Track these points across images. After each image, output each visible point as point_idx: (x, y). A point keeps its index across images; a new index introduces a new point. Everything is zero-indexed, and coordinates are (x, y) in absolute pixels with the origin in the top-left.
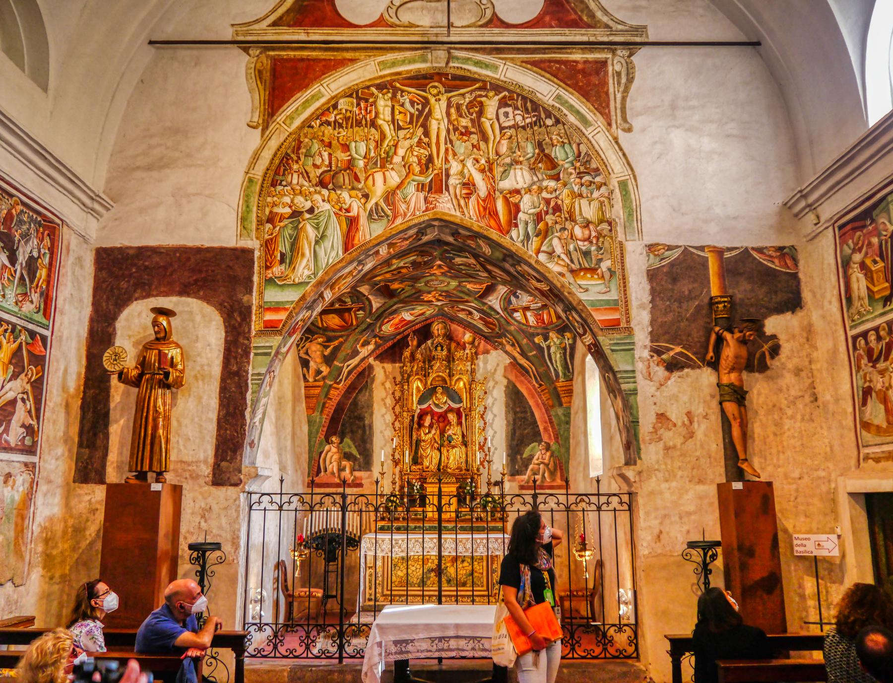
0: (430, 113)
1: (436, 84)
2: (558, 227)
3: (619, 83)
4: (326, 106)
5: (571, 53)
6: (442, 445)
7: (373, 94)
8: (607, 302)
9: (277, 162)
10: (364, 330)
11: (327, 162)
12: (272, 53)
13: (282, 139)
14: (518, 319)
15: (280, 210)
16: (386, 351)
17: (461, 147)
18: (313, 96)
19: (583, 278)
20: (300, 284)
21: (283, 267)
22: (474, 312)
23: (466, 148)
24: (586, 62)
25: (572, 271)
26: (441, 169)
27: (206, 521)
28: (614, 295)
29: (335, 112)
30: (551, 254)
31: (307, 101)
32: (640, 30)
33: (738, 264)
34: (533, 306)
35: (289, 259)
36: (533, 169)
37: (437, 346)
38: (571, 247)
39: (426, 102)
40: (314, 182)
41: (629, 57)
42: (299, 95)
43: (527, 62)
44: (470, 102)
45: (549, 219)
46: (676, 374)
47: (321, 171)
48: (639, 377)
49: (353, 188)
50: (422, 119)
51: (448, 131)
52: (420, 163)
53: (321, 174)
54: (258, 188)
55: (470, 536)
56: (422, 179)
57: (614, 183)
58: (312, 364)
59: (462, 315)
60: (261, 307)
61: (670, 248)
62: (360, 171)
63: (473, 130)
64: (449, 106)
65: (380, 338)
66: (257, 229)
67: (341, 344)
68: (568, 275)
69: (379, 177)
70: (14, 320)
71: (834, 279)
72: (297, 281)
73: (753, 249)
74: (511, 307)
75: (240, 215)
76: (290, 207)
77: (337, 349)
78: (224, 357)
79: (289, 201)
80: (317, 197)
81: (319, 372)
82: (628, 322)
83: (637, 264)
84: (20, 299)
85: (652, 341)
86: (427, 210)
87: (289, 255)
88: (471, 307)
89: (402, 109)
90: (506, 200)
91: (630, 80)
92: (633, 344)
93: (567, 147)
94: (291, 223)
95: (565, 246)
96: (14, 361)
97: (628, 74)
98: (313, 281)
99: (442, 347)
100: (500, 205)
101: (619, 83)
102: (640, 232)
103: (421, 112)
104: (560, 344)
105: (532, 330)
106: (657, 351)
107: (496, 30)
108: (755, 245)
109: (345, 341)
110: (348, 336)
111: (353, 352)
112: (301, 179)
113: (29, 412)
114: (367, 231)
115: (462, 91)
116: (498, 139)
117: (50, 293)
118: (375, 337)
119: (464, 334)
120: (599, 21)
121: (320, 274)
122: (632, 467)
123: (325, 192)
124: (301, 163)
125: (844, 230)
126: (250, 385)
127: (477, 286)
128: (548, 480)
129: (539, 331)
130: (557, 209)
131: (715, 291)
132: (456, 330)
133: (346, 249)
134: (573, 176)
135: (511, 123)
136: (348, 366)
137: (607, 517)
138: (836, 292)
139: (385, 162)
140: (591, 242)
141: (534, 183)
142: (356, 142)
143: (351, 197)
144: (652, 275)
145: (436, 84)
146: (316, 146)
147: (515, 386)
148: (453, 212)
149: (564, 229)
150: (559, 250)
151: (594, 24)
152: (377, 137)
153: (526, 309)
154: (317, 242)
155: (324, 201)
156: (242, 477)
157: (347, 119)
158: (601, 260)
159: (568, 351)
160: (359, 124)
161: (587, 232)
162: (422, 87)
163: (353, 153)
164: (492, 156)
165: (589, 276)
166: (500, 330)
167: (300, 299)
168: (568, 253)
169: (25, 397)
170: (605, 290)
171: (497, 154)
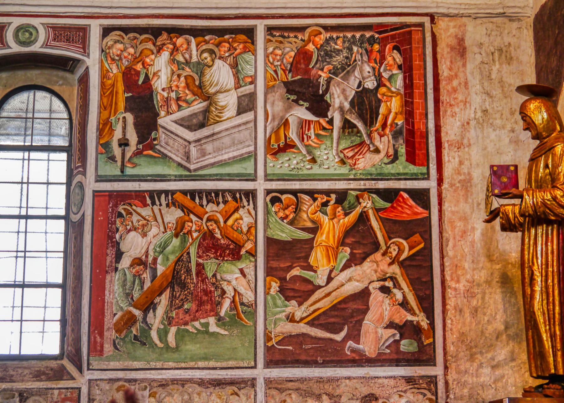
70: (341, 185)
84: (350, 154)
96: (349, 241)
113: (404, 304)
117: (419, 126)
169: (389, 284)
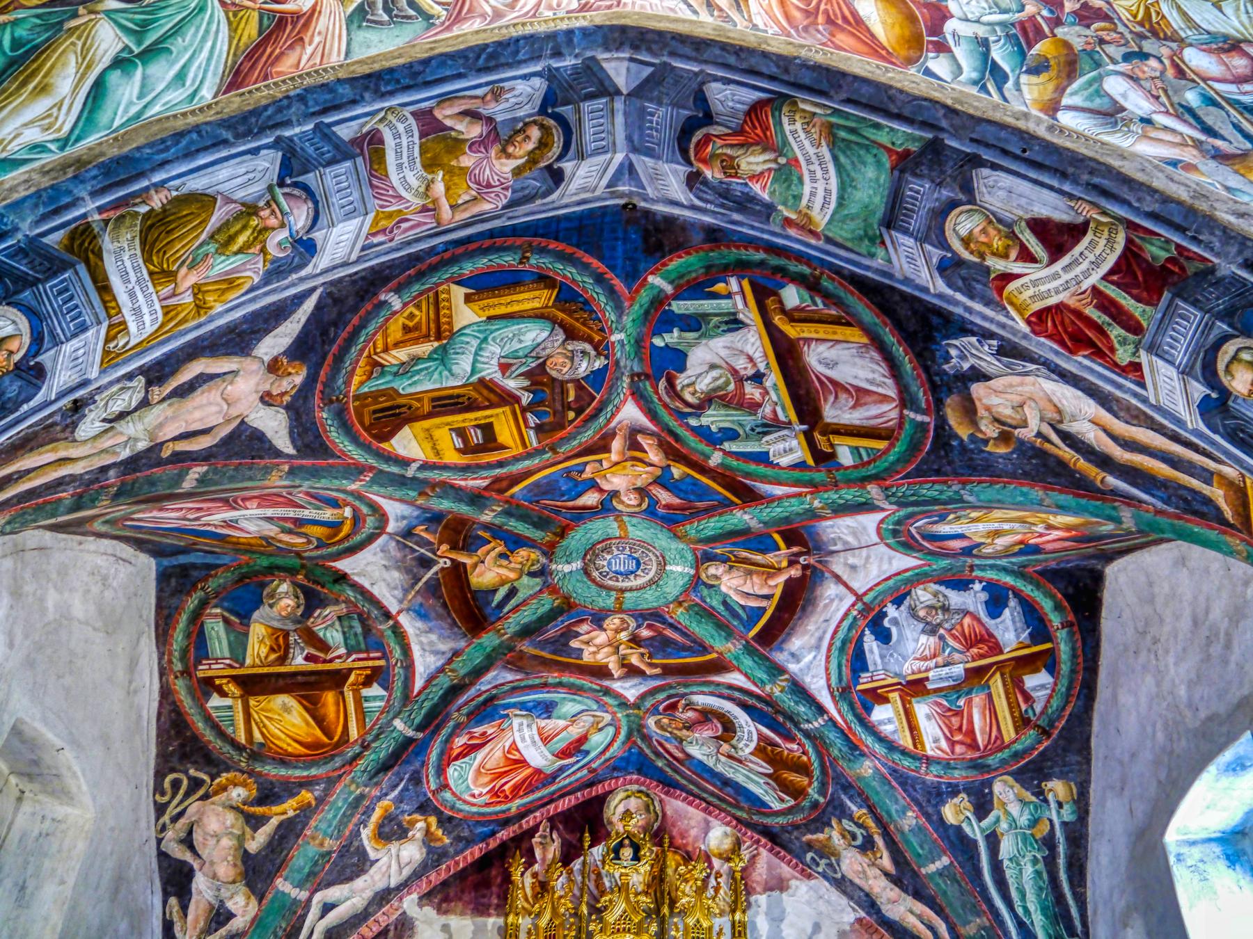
10: (385, 767)
14: (887, 729)
16: (462, 875)
22: (742, 718)
30: (1112, 114)
34: (938, 676)
37: (621, 845)
58: (200, 883)
59: (700, 748)
65: (444, 821)
67: (306, 812)
74: (865, 683)
77: (289, 832)
81: (220, 916)
88: (731, 692)
99: (637, 849)
104: (1034, 822)
105: (931, 775)
109: (320, 801)
110: (331, 782)
111: (344, 851)
118: (424, 808)
119: (707, 829)
127: (755, 585)
129: (958, 775)
132: (680, 815)
136: (327, 908)
153: (915, 687)
159: (1061, 849)
166: (822, 792)
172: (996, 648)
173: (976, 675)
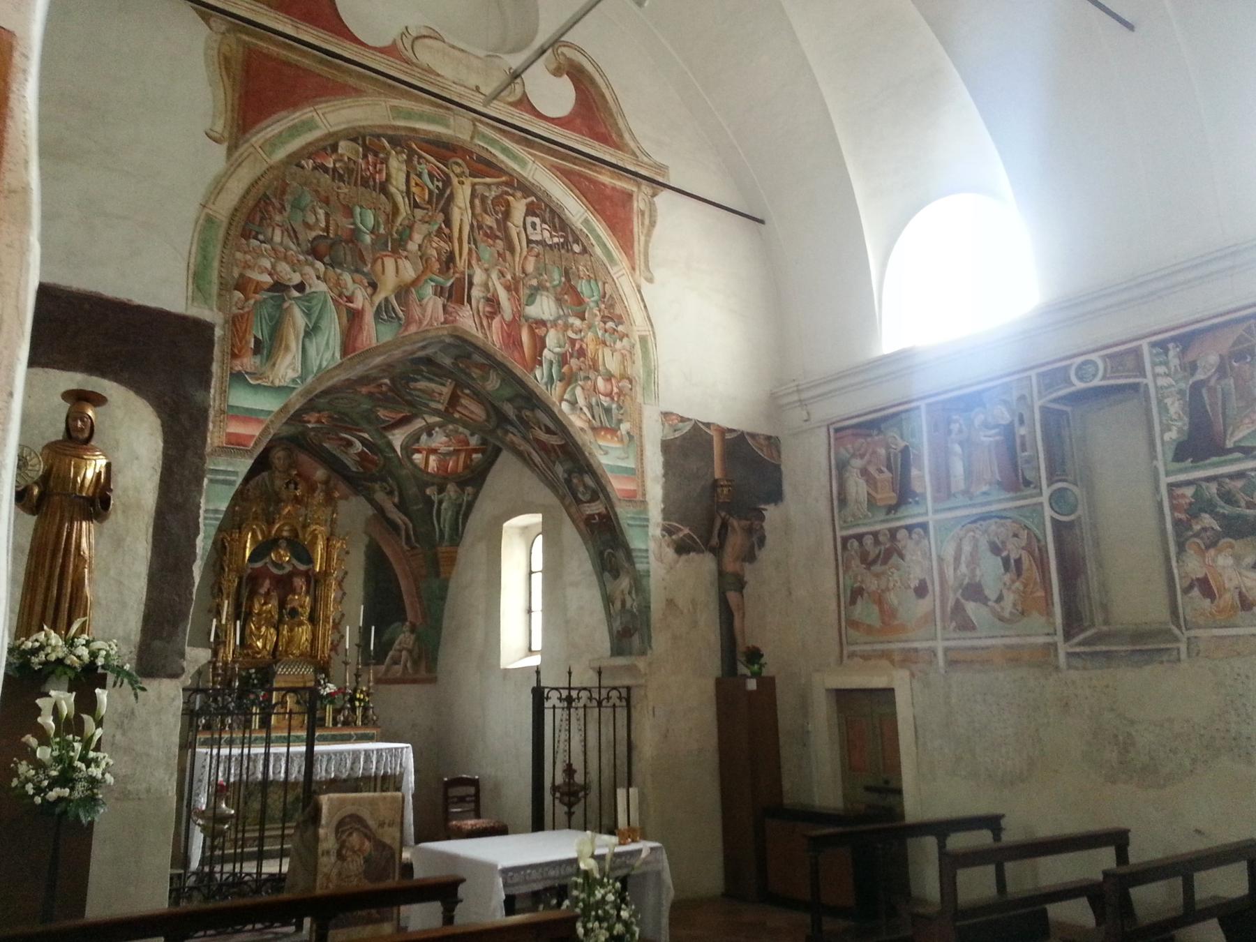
0: (451, 198)
1: (460, 161)
2: (582, 374)
3: (643, 224)
4: (322, 144)
5: (600, 173)
6: (281, 621)
7: (384, 148)
8: (626, 469)
9: (251, 203)
11: (323, 225)
12: (245, 38)
13: (258, 172)
14: (417, 461)
15: (255, 276)
17: (487, 252)
18: (304, 123)
19: (604, 438)
20: (280, 389)
21: (257, 360)
23: (491, 255)
24: (614, 188)
25: (593, 429)
26: (463, 273)
27: (124, 734)
28: (631, 464)
29: (334, 157)
31: (294, 127)
32: (662, 168)
33: (739, 446)
35: (268, 348)
36: (559, 301)
38: (594, 401)
39: (447, 182)
40: (305, 248)
41: (654, 195)
42: (283, 113)
43: (558, 169)
44: (496, 197)
45: (574, 362)
46: (684, 557)
47: (314, 234)
48: (652, 558)
49: (357, 271)
50: (443, 201)
51: (472, 226)
52: (439, 260)
53: (314, 239)
54: (221, 233)
55: (284, 750)
56: (440, 279)
57: (635, 337)
60: (223, 412)
61: (683, 420)
62: (366, 249)
63: (498, 234)
64: (473, 195)
66: (220, 295)
68: (589, 432)
69: (389, 263)
71: (824, 479)
72: (277, 383)
73: (748, 434)
75: (192, 266)
76: (270, 274)
78: (161, 480)
79: (269, 266)
80: (308, 269)
82: (644, 495)
83: (653, 434)
85: (664, 519)
86: (446, 322)
87: (267, 343)
89: (419, 181)
90: (531, 330)
91: (653, 224)
92: (647, 520)
93: (593, 282)
94: (272, 298)
95: (587, 398)
97: (651, 216)
98: (300, 388)
100: (525, 337)
101: (643, 224)
102: (657, 397)
103: (442, 192)
105: (425, 478)
106: (668, 531)
107: (527, 116)
108: (749, 430)
112: (287, 241)
114: (374, 334)
115: (488, 180)
116: (525, 253)
120: (627, 145)
121: (310, 379)
122: (643, 658)
123: (319, 265)
124: (286, 214)
125: (839, 435)
126: (201, 526)
128: (410, 671)
129: (436, 480)
130: (582, 353)
131: (718, 474)
133: (344, 352)
134: (598, 318)
135: (538, 238)
137: (606, 712)
138: (826, 490)
139: (398, 245)
140: (612, 399)
141: (559, 317)
142: (361, 207)
143: (354, 281)
144: (666, 447)
145: (460, 161)
146: (308, 198)
147: (379, 548)
148: (474, 331)
149: (587, 378)
150: (581, 402)
151: (619, 146)
152: (389, 209)
154: (308, 334)
155: (318, 278)
156: (185, 664)
157: (350, 171)
158: (620, 421)
160: (365, 183)
161: (609, 387)
162: (443, 159)
163: (358, 221)
164: (519, 273)
165: (609, 436)
167: (281, 410)
168: (590, 407)
170: (623, 455)
171: (524, 271)
172: (468, 444)
173: (457, 452)
